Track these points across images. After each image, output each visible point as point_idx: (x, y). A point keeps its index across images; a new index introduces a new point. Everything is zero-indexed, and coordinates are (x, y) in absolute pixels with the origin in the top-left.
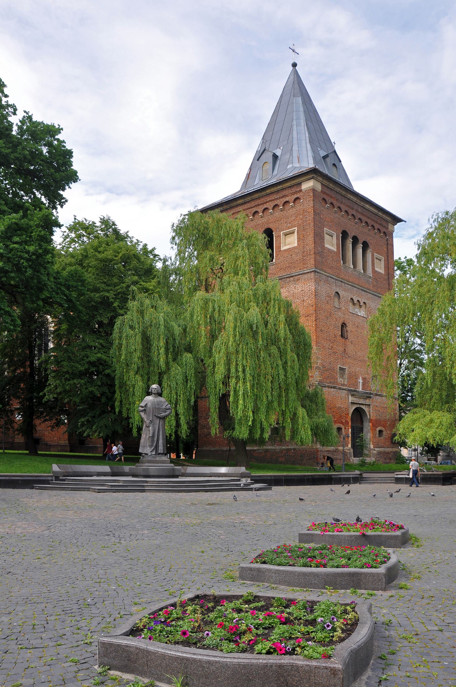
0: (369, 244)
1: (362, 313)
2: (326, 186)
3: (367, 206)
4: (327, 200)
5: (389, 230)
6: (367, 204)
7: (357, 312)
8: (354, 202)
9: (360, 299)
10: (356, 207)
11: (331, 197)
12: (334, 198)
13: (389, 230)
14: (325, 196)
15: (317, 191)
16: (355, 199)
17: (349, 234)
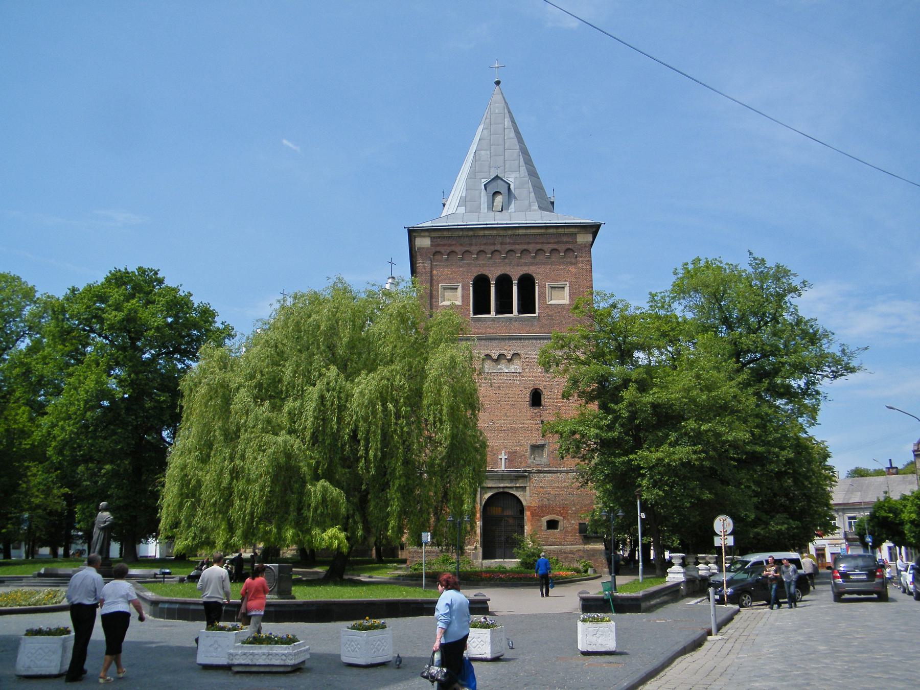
0: (534, 275)
1: (515, 367)
2: (439, 237)
3: (521, 232)
4: (443, 251)
5: (578, 243)
6: (518, 230)
7: (501, 369)
8: (494, 236)
9: (505, 352)
10: (500, 239)
11: (450, 245)
12: (455, 244)
13: (578, 243)
14: (438, 249)
15: (423, 248)
16: (495, 232)
17: (490, 276)
